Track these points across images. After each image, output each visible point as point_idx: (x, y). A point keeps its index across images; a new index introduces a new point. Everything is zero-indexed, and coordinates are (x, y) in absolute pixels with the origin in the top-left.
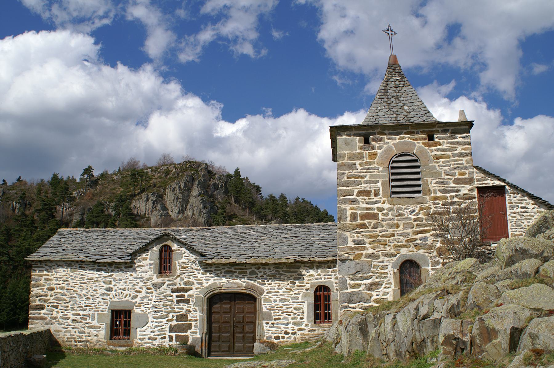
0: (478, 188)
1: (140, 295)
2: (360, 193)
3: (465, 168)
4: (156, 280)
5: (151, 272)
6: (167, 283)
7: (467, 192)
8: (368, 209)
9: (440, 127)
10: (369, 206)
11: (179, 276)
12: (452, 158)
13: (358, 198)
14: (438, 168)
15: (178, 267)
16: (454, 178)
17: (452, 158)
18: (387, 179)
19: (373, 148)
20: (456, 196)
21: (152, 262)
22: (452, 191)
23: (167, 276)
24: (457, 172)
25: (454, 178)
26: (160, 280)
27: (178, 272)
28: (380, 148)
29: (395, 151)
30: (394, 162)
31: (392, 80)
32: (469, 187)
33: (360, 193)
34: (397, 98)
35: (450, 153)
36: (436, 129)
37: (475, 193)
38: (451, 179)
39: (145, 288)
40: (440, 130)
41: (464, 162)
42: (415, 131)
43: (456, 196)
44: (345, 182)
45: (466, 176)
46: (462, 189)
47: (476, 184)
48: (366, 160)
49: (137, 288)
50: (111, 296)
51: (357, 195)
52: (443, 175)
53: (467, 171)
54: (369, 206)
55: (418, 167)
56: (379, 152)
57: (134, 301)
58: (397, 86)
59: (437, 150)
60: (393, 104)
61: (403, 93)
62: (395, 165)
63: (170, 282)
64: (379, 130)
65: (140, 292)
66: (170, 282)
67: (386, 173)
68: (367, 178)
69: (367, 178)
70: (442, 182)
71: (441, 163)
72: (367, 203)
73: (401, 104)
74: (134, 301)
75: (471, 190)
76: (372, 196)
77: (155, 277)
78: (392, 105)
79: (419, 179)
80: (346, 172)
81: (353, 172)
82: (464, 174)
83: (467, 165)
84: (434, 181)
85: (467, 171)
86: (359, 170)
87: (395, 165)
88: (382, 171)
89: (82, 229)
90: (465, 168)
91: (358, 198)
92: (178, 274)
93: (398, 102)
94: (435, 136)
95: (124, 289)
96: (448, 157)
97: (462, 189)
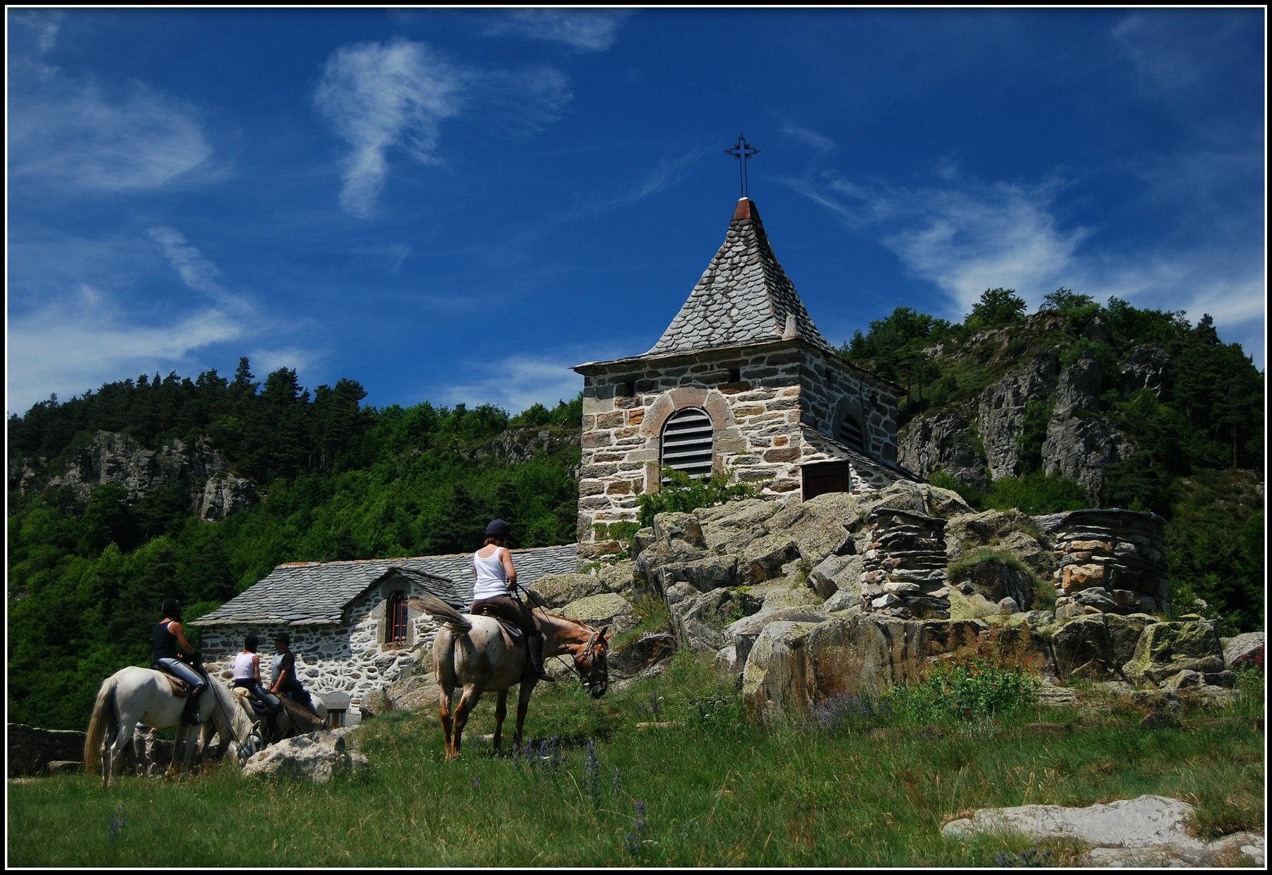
0: (803, 467)
1: (359, 682)
2: (614, 488)
3: (787, 429)
4: (382, 655)
5: (374, 641)
6: (400, 659)
7: (785, 475)
8: (624, 516)
9: (749, 354)
10: (626, 510)
11: (418, 646)
12: (767, 413)
13: (609, 497)
14: (740, 432)
15: (416, 630)
16: (766, 450)
17: (767, 413)
18: (656, 459)
19: (638, 404)
20: (768, 485)
21: (376, 622)
22: (761, 476)
23: (399, 647)
24: (772, 438)
25: (766, 450)
26: (387, 655)
27: (417, 639)
28: (649, 402)
29: (673, 407)
30: (671, 427)
31: (730, 254)
32: (789, 466)
33: (614, 488)
34: (725, 292)
35: (763, 403)
36: (743, 358)
37: (799, 479)
38: (760, 453)
39: (365, 670)
40: (750, 358)
41: (785, 419)
42: (708, 364)
43: (768, 485)
44: (591, 469)
45: (786, 446)
46: (779, 471)
47: (803, 460)
48: (627, 426)
49: (354, 670)
50: (316, 686)
51: (609, 492)
52: (749, 445)
53: (789, 437)
54: (626, 510)
55: (709, 434)
56: (647, 408)
57: (350, 693)
58: (734, 266)
59: (743, 399)
60: (715, 307)
61: (738, 281)
62: (669, 433)
63: (403, 658)
64: (648, 369)
65: (356, 676)
66: (403, 658)
67: (656, 450)
68: (625, 460)
69: (625, 460)
70: (746, 459)
71: (747, 424)
72: (623, 506)
73: (729, 305)
74: (350, 693)
75: (793, 472)
76: (632, 494)
77: (379, 649)
78: (712, 308)
79: (708, 457)
80: (594, 450)
81: (605, 451)
82: (783, 442)
83: (790, 425)
84: (733, 459)
85: (789, 437)
86: (614, 446)
87: (669, 433)
88: (649, 446)
89: (315, 564)
90: (787, 429)
91: (609, 497)
92: (415, 643)
93: (725, 300)
94: (742, 372)
95: (334, 673)
96: (760, 410)
97: (779, 471)
